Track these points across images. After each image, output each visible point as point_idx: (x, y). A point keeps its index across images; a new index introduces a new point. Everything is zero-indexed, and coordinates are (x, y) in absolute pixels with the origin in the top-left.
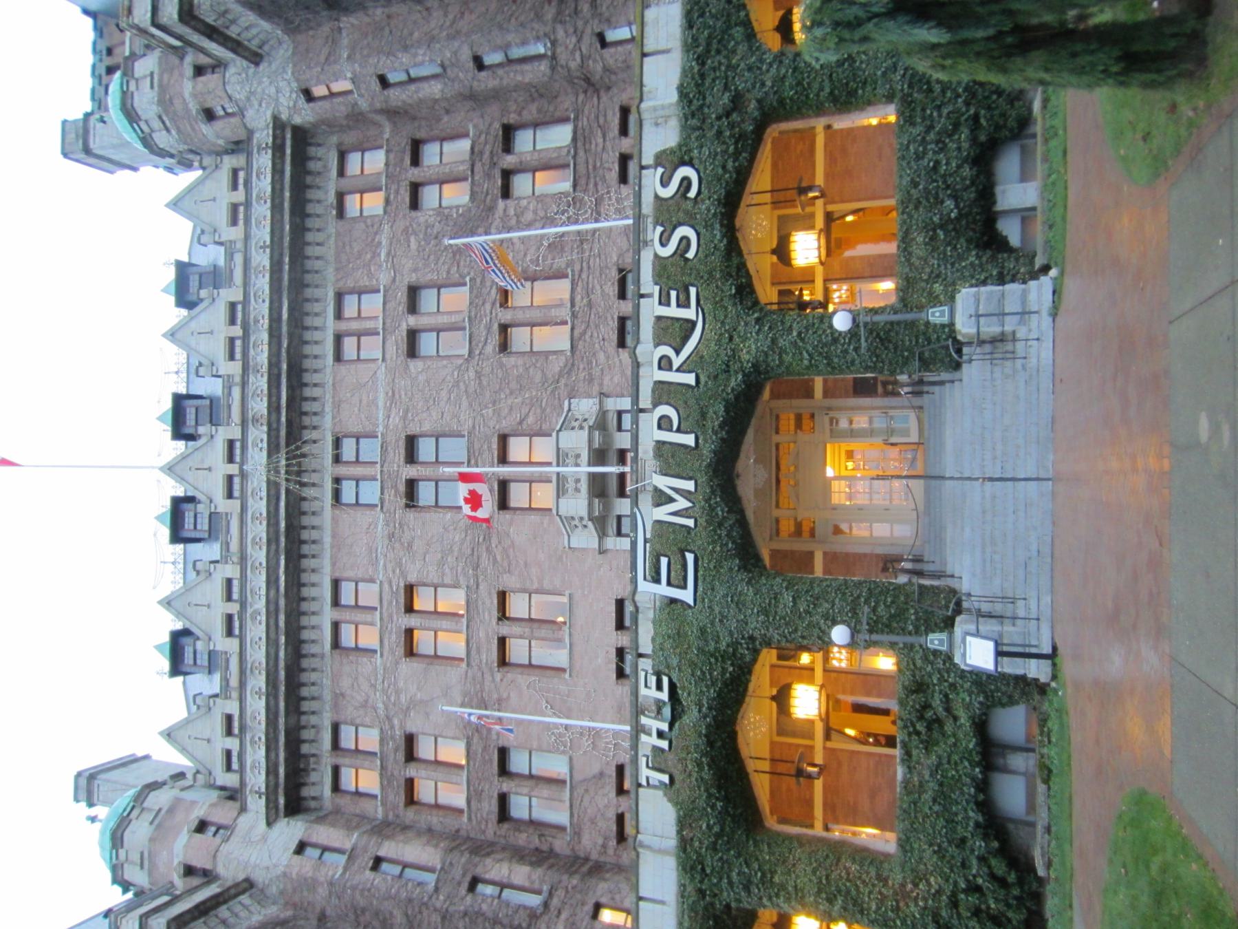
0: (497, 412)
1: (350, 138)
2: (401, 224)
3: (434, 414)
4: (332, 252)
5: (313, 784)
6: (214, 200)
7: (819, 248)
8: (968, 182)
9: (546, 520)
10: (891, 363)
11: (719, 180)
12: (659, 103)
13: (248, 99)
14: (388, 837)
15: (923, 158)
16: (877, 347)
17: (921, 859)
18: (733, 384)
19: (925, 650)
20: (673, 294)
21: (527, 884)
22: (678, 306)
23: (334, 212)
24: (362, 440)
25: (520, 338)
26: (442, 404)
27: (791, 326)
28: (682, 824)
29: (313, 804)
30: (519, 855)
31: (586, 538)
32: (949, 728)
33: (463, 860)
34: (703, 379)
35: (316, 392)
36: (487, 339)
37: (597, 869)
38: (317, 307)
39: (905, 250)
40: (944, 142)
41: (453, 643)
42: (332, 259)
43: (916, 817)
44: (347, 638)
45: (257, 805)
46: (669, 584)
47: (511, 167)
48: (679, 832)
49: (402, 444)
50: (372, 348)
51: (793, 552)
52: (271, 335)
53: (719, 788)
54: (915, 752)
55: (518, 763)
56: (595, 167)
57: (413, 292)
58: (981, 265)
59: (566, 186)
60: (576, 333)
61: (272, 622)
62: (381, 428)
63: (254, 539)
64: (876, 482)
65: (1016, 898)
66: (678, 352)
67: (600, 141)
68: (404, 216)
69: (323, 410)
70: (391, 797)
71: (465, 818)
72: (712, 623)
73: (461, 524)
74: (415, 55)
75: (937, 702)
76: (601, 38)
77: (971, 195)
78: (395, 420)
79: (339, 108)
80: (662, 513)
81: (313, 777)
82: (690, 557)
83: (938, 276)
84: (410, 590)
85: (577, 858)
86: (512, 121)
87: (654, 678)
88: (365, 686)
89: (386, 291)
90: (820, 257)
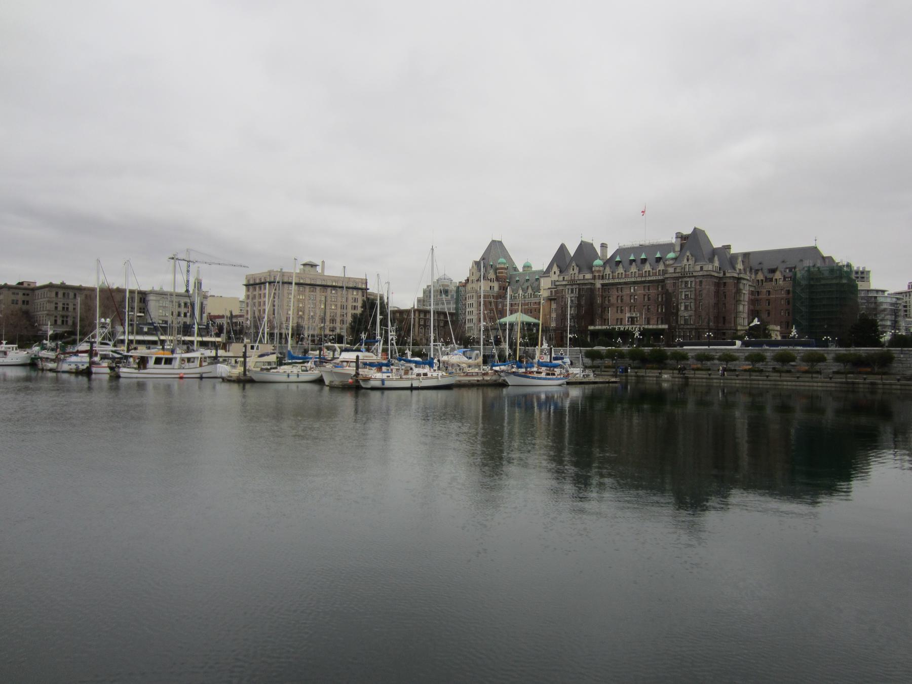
30: (601, 310)
37: (602, 317)
45: (601, 282)
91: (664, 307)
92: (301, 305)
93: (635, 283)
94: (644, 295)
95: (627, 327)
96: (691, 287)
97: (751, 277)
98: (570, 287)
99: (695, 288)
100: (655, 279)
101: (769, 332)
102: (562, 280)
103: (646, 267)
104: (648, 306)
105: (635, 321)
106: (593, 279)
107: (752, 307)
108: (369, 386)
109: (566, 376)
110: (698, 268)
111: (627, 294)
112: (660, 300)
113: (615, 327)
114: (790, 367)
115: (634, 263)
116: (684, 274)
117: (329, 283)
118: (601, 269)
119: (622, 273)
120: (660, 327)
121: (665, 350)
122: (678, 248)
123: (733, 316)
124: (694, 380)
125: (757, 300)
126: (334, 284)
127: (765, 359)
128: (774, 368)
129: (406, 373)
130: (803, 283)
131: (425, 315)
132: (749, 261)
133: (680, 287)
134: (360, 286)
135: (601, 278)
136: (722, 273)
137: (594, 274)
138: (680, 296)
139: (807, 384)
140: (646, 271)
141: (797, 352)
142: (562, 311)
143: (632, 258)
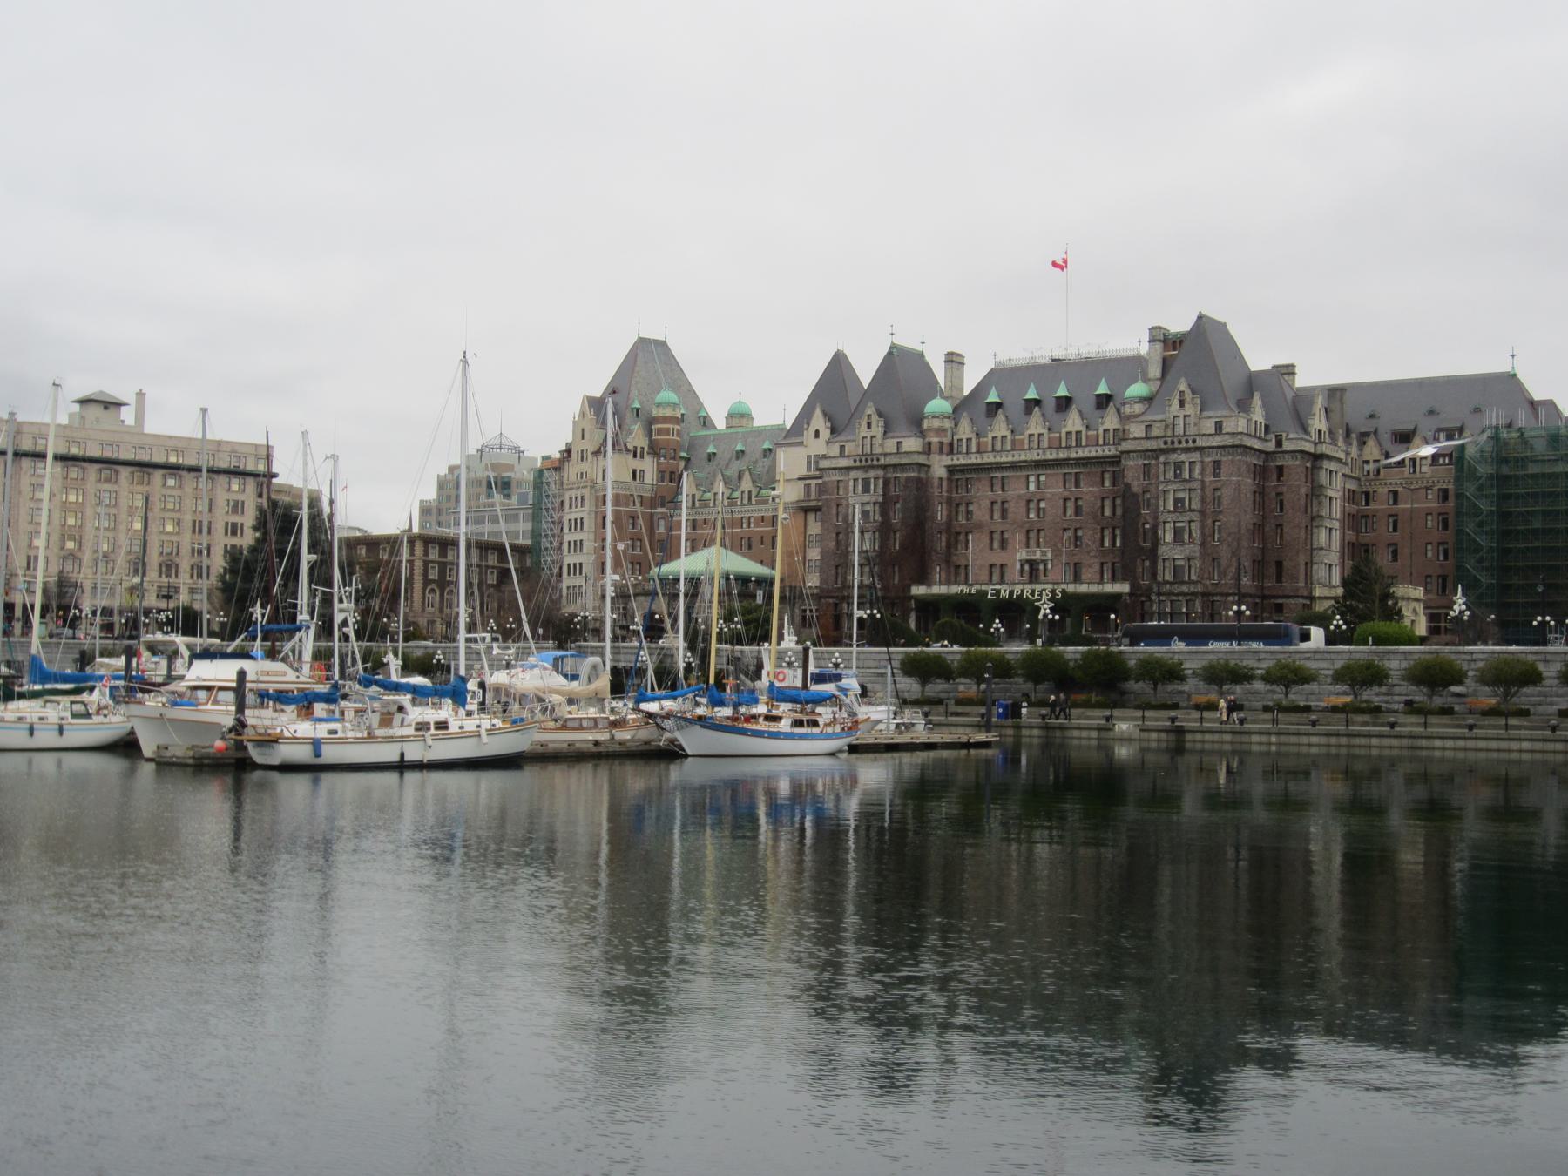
37: (948, 562)
45: (948, 460)
78: (1049, 496)
91: (1118, 532)
92: (71, 521)
93: (1039, 465)
94: (1065, 500)
95: (1018, 589)
96: (1191, 479)
97: (1347, 453)
98: (860, 475)
99: (1203, 481)
100: (1093, 454)
101: (1396, 603)
102: (838, 454)
103: (1070, 422)
104: (1076, 530)
105: (1042, 573)
106: (923, 453)
107: (1351, 536)
108: (276, 762)
109: (850, 728)
110: (1209, 426)
111: (1020, 496)
112: (1108, 512)
113: (984, 587)
114: (1450, 699)
115: (1037, 409)
116: (1173, 443)
117: (158, 458)
118: (947, 424)
119: (1004, 437)
120: (1109, 588)
121: (1121, 652)
122: (1155, 371)
123: (1302, 559)
124: (1198, 737)
125: (1367, 516)
126: (173, 459)
127: (1387, 676)
128: (1409, 703)
129: (386, 721)
130: (1483, 470)
131: (443, 553)
132: (1342, 409)
133: (1162, 479)
134: (250, 467)
135: (946, 449)
136: (1274, 440)
137: (927, 440)
138: (1161, 503)
139: (1494, 745)
140: (1069, 433)
141: (1468, 657)
142: (838, 542)
143: (1032, 394)
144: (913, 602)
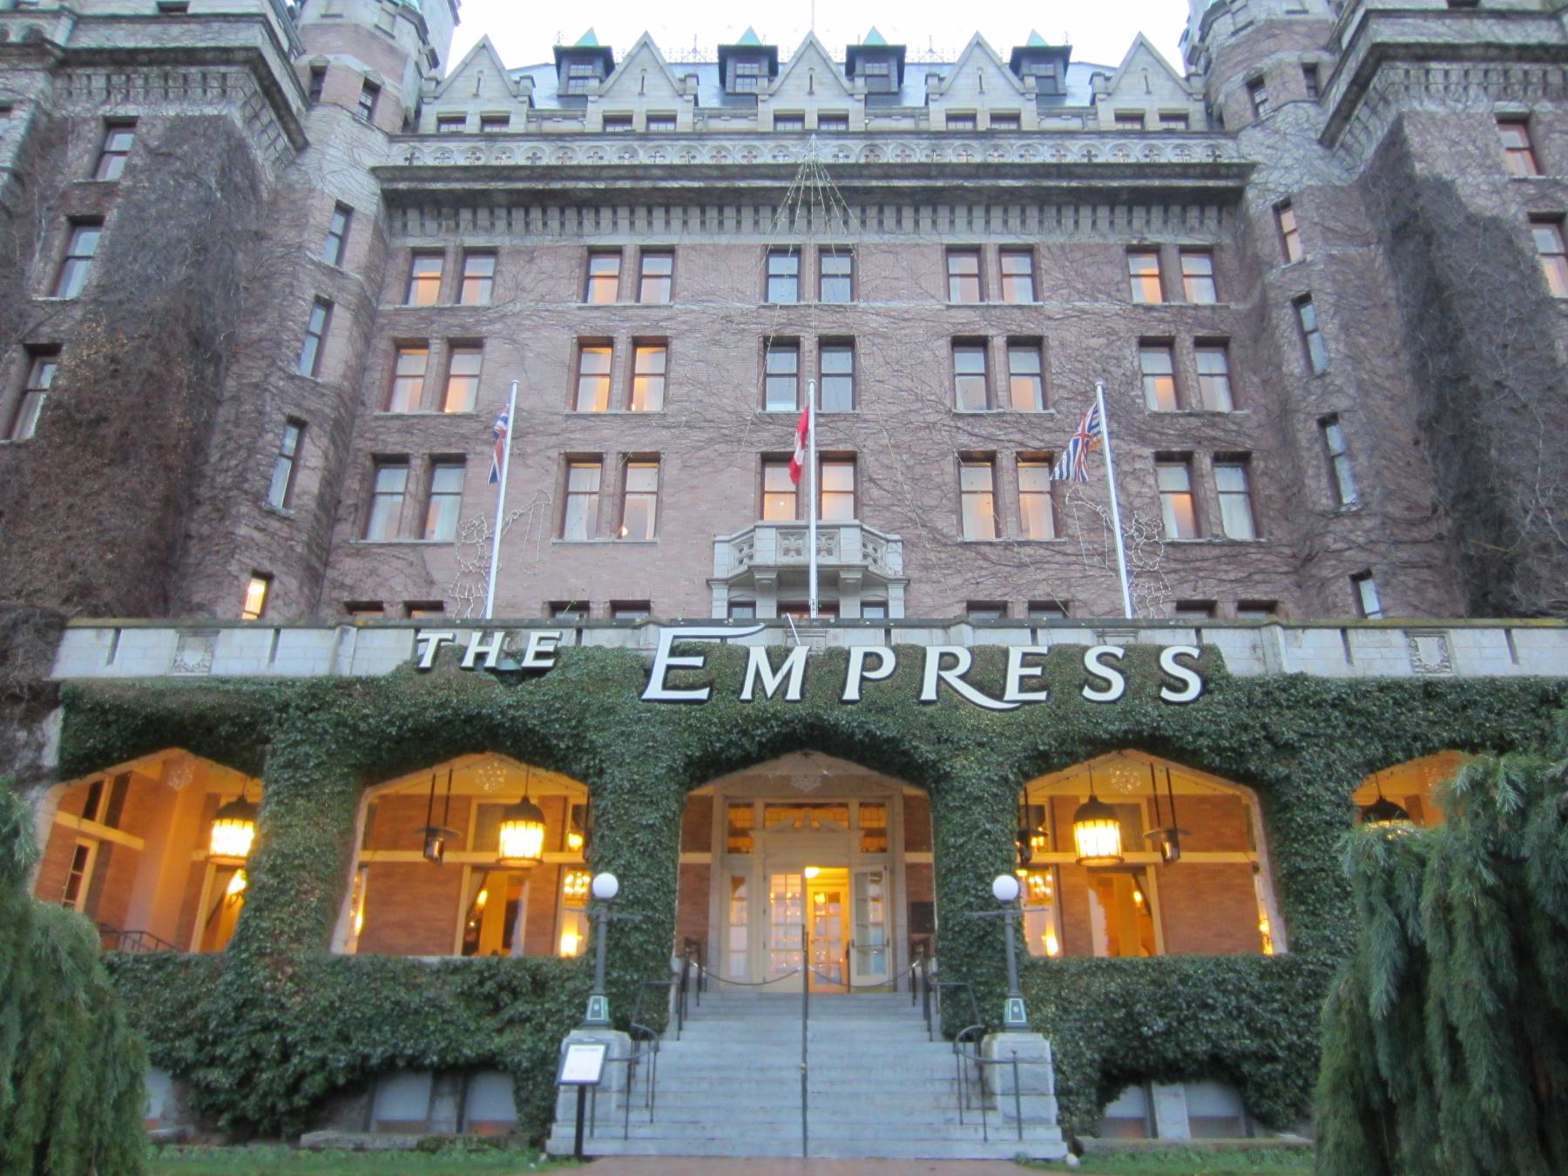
0: (884, 450)
1: (1229, 260)
2: (1120, 325)
3: (881, 371)
4: (1084, 240)
5: (422, 225)
6: (1148, 92)
7: (1099, 857)
8: (1188, 1048)
9: (749, 513)
10: (952, 949)
11: (1184, 728)
12: (1283, 652)
13: (1276, 132)
14: (356, 318)
15: (1218, 990)
16: (972, 931)
17: (324, 985)
18: (924, 747)
19: (587, 993)
20: (1037, 671)
21: (297, 490)
22: (1022, 678)
23: (1135, 242)
24: (848, 281)
25: (978, 477)
26: (894, 381)
27: (997, 821)
28: (369, 683)
29: (398, 224)
30: (332, 480)
31: (725, 563)
32: (490, 1023)
33: (327, 411)
34: (929, 709)
35: (908, 223)
36: (976, 435)
37: (314, 578)
38: (1014, 222)
39: (1099, 967)
40: (1239, 1016)
41: (595, 397)
42: (1075, 240)
43: (375, 979)
44: (601, 266)
46: (669, 668)
47: (1196, 464)
48: (359, 680)
49: (843, 331)
50: (964, 292)
51: (710, 824)
52: (978, 166)
53: (414, 731)
54: (457, 979)
55: (446, 479)
56: (1198, 569)
57: (1035, 343)
58: (1081, 1066)
59: (1173, 533)
60: (986, 549)
61: (622, 172)
62: (863, 305)
63: (725, 148)
64: (799, 932)
65: (274, 1106)
66: (962, 677)
67: (1232, 576)
68: (1132, 330)
69: (884, 232)
70: (405, 321)
71: (378, 413)
72: (620, 722)
73: (743, 407)
74: (1336, 340)
75: (522, 1007)
76: (1365, 575)
77: (1171, 1052)
78: (874, 322)
79: (1267, 247)
80: (758, 658)
81: (431, 225)
82: (703, 694)
83: (1065, 1010)
84: (661, 343)
85: (329, 554)
86: (1254, 463)
87: (551, 648)
88: (542, 289)
89: (1036, 309)
90: (1088, 858)
135: (387, 115)
144: (53, 726)
